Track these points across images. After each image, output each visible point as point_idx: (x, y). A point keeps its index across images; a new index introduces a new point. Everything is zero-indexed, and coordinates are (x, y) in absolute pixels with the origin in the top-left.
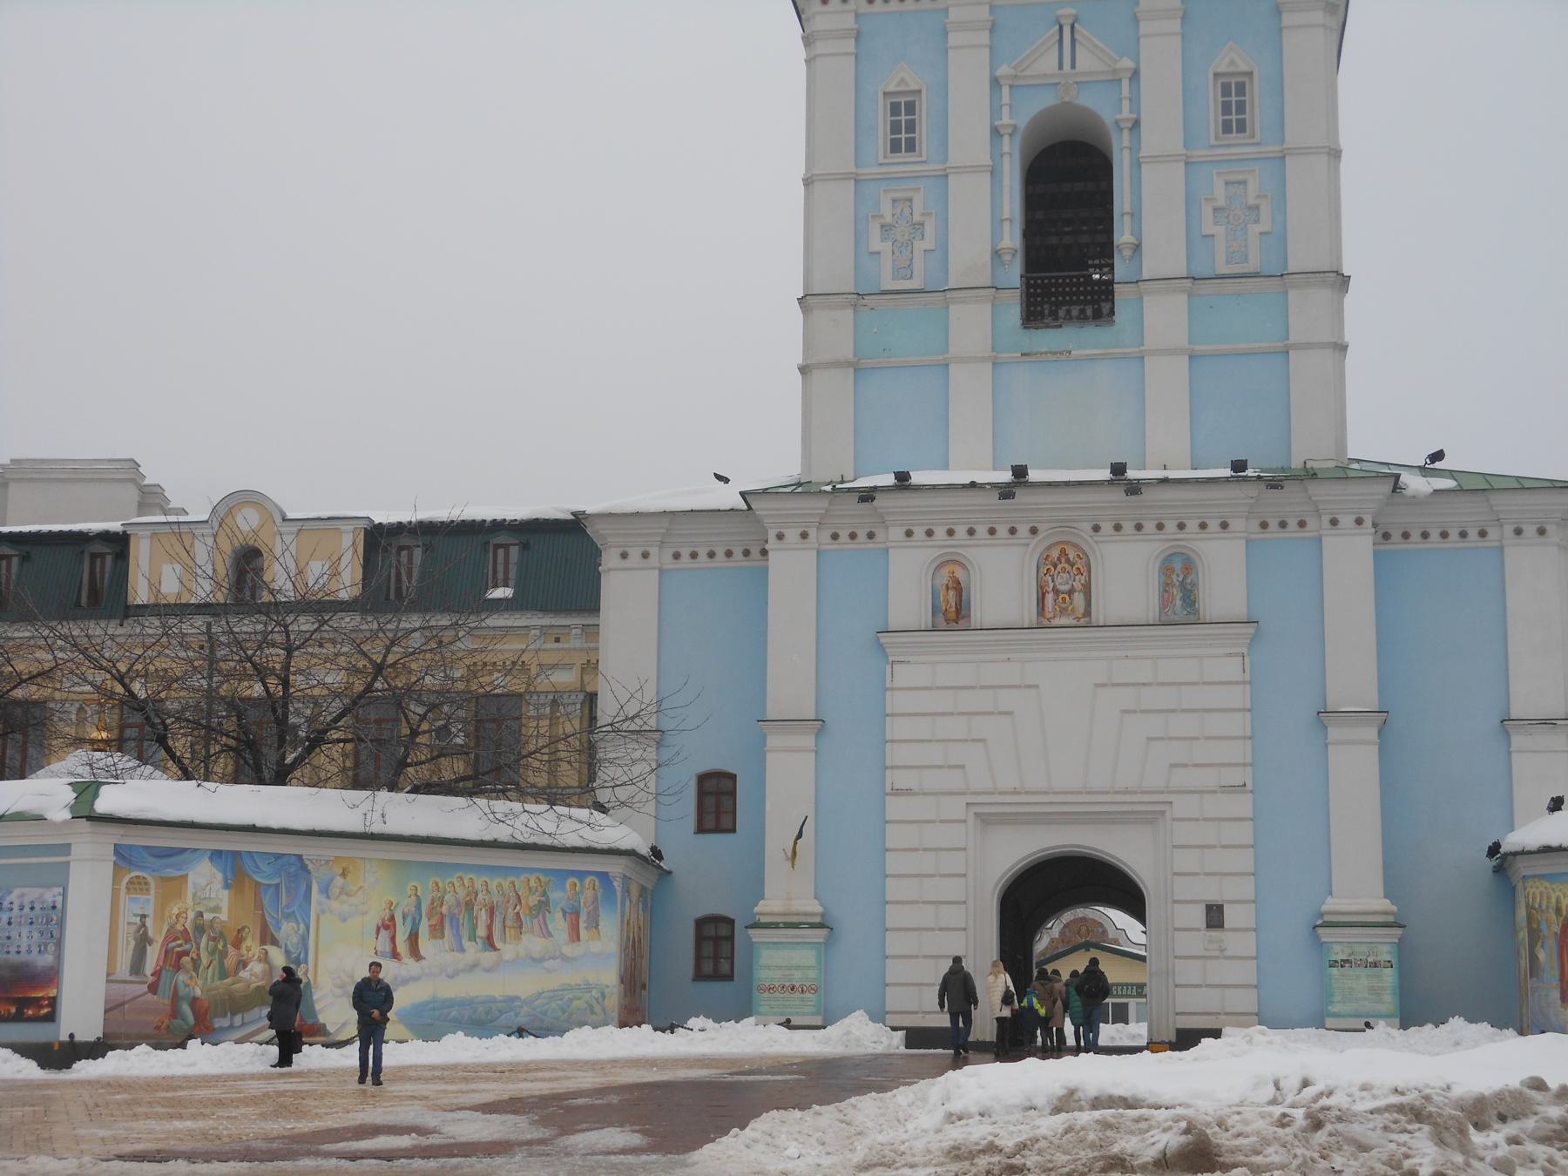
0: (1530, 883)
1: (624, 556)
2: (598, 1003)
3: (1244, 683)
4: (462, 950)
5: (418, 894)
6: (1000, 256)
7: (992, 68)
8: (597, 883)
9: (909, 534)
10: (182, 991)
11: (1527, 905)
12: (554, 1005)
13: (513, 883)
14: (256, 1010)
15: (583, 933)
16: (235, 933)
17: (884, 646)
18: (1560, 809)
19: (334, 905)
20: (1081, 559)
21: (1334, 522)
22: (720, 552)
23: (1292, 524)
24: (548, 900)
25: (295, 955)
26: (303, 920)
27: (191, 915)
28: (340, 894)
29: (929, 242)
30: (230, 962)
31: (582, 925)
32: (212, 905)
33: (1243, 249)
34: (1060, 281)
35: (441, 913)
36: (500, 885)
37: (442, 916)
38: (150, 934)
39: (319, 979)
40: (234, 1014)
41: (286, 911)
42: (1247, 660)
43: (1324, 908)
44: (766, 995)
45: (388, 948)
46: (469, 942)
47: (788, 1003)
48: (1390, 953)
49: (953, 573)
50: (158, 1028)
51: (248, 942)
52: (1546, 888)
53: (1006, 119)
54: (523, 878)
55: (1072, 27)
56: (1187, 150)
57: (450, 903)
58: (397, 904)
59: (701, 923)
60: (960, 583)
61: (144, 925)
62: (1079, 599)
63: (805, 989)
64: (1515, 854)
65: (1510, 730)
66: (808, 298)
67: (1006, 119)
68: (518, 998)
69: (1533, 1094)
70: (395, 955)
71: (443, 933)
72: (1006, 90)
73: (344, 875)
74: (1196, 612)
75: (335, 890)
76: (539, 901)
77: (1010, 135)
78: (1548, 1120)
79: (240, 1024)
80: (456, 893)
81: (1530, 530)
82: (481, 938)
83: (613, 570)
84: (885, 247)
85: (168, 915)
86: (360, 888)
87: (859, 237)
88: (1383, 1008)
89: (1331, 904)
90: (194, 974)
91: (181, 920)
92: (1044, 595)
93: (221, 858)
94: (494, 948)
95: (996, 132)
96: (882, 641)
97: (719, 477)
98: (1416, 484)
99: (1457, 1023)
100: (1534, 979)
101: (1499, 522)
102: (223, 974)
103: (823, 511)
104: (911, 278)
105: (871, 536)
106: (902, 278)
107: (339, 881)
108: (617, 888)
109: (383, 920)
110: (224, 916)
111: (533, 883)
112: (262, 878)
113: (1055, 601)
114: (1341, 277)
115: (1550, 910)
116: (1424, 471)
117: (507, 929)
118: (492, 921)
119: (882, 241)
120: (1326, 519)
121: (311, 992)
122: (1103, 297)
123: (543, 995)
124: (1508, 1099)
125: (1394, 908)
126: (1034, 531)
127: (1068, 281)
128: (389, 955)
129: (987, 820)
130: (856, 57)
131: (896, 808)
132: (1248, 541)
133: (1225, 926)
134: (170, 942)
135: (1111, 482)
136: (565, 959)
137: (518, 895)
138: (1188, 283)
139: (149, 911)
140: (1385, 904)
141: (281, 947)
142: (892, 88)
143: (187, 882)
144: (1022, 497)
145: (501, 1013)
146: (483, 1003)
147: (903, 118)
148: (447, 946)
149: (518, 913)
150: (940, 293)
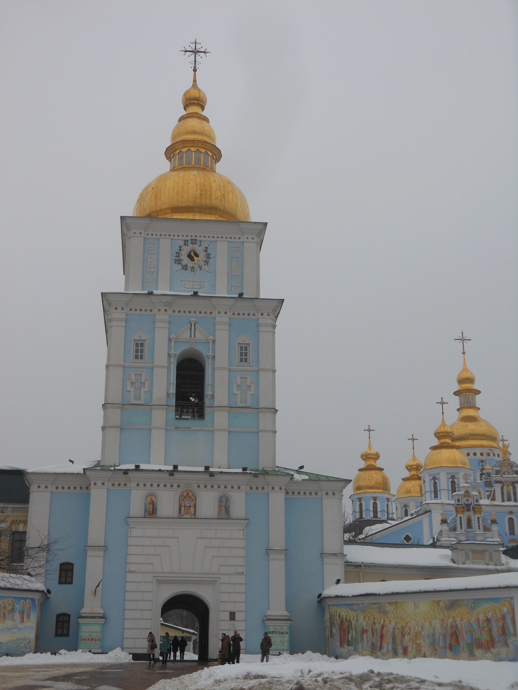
0: (331, 607)
1: (39, 487)
3: (244, 539)
6: (169, 395)
7: (169, 335)
8: (31, 602)
9: (138, 485)
11: (330, 614)
13: (4, 602)
15: (25, 620)
17: (128, 522)
18: (339, 583)
20: (193, 496)
21: (273, 488)
22: (72, 487)
23: (260, 488)
29: (146, 389)
31: (25, 616)
33: (245, 399)
34: (185, 404)
42: (245, 531)
43: (267, 614)
44: (83, 642)
47: (90, 645)
48: (287, 629)
49: (152, 499)
52: (336, 609)
53: (173, 352)
55: (195, 324)
56: (229, 366)
59: (58, 616)
60: (154, 502)
62: (192, 509)
63: (96, 640)
64: (327, 598)
65: (324, 557)
66: (106, 404)
67: (173, 352)
69: (371, 674)
72: (173, 343)
74: (229, 515)
77: (174, 357)
78: (376, 681)
81: (330, 493)
83: (35, 492)
84: (132, 389)
87: (124, 386)
88: (285, 648)
89: (269, 613)
92: (181, 507)
95: (169, 355)
96: (128, 520)
97: (70, 461)
98: (297, 477)
99: (309, 653)
100: (332, 638)
101: (321, 490)
103: (110, 476)
104: (140, 400)
105: (125, 485)
106: (137, 400)
108: (37, 603)
113: (185, 509)
114: (275, 410)
115: (337, 616)
116: (298, 472)
119: (131, 387)
120: (271, 487)
122: (190, 407)
123: (11, 642)
124: (366, 676)
125: (289, 614)
126: (179, 486)
127: (188, 404)
129: (160, 582)
130: (125, 328)
131: (130, 577)
132: (246, 493)
133: (236, 620)
135: (204, 472)
136: (19, 629)
138: (228, 409)
140: (286, 613)
142: (136, 338)
144: (176, 475)
147: (140, 348)
149: (4, 613)
150: (149, 406)
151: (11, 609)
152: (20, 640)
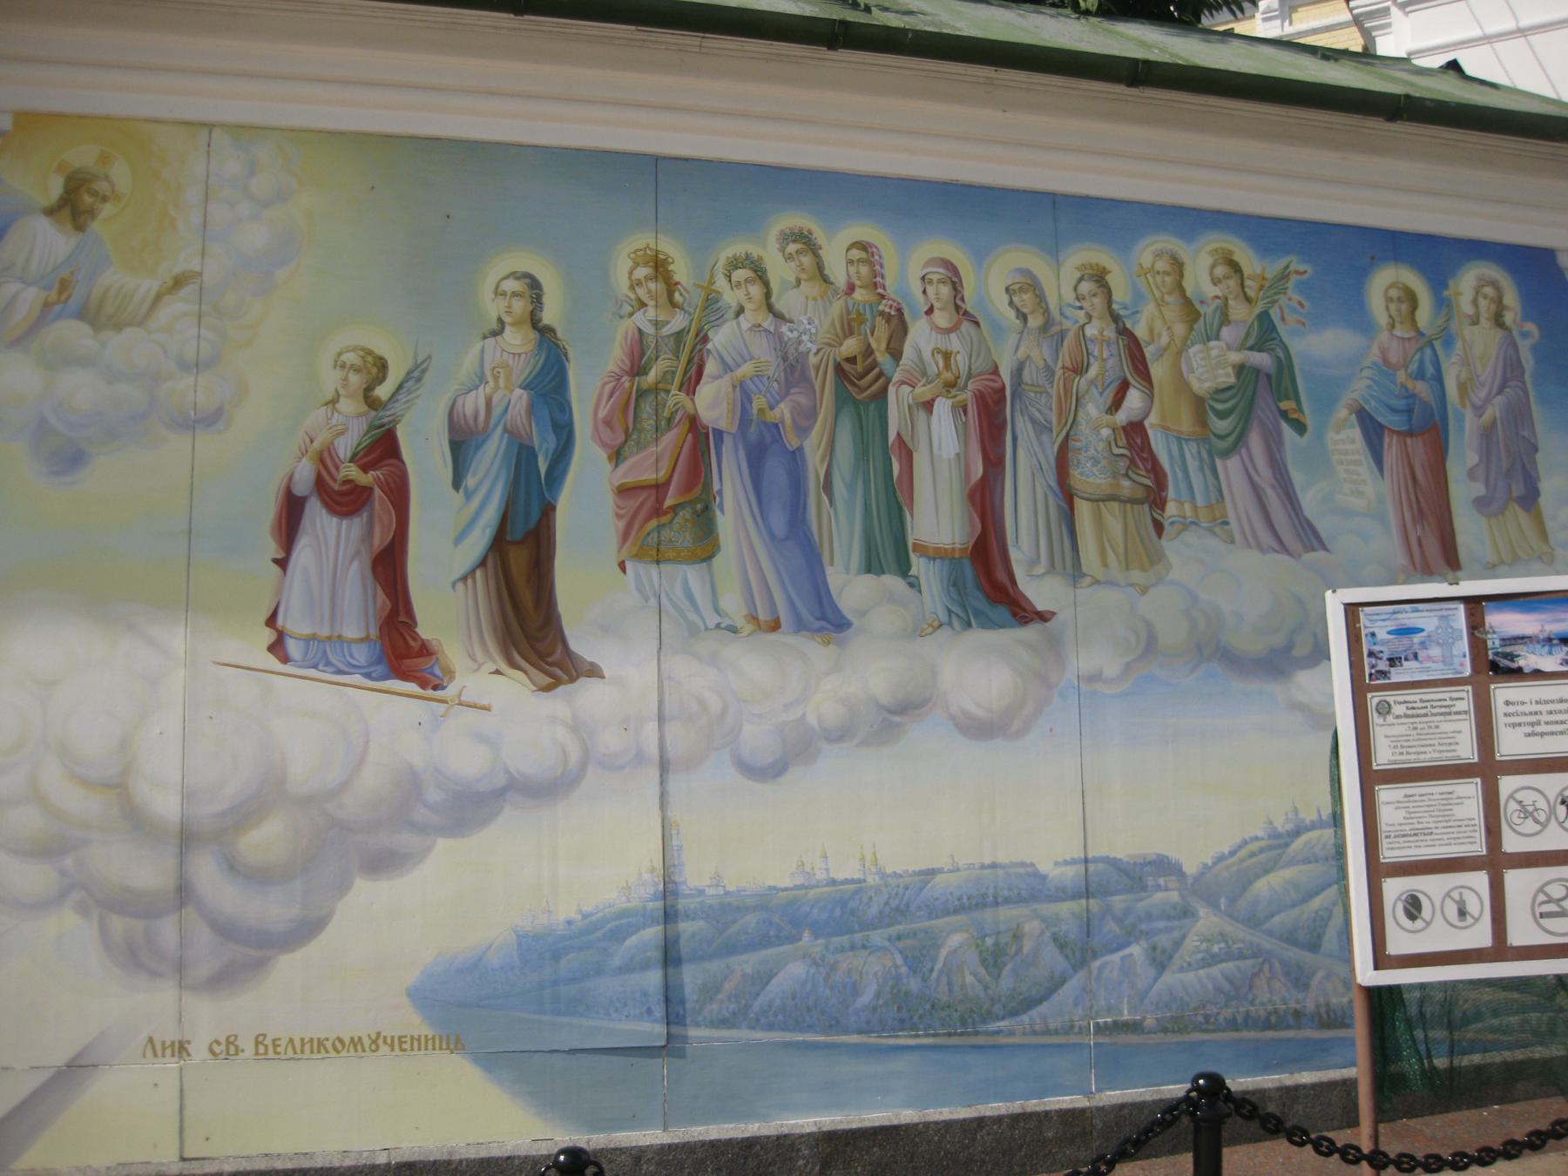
5: (549, 316)
8: (1511, 298)
13: (1100, 278)
15: (1469, 528)
24: (1285, 367)
28: (46, 313)
31: (1462, 491)
35: (694, 422)
36: (1032, 285)
37: (700, 438)
46: (869, 579)
54: (1150, 249)
57: (746, 369)
58: (415, 374)
68: (1164, 866)
76: (1240, 369)
80: (778, 316)
82: (934, 554)
86: (178, 283)
94: (1022, 612)
109: (325, 459)
111: (1201, 278)
117: (1083, 509)
118: (994, 463)
123: (1298, 843)
128: (361, 655)
137: (1124, 332)
146: (974, 902)
148: (733, 604)
149: (1135, 430)
151: (1227, 377)
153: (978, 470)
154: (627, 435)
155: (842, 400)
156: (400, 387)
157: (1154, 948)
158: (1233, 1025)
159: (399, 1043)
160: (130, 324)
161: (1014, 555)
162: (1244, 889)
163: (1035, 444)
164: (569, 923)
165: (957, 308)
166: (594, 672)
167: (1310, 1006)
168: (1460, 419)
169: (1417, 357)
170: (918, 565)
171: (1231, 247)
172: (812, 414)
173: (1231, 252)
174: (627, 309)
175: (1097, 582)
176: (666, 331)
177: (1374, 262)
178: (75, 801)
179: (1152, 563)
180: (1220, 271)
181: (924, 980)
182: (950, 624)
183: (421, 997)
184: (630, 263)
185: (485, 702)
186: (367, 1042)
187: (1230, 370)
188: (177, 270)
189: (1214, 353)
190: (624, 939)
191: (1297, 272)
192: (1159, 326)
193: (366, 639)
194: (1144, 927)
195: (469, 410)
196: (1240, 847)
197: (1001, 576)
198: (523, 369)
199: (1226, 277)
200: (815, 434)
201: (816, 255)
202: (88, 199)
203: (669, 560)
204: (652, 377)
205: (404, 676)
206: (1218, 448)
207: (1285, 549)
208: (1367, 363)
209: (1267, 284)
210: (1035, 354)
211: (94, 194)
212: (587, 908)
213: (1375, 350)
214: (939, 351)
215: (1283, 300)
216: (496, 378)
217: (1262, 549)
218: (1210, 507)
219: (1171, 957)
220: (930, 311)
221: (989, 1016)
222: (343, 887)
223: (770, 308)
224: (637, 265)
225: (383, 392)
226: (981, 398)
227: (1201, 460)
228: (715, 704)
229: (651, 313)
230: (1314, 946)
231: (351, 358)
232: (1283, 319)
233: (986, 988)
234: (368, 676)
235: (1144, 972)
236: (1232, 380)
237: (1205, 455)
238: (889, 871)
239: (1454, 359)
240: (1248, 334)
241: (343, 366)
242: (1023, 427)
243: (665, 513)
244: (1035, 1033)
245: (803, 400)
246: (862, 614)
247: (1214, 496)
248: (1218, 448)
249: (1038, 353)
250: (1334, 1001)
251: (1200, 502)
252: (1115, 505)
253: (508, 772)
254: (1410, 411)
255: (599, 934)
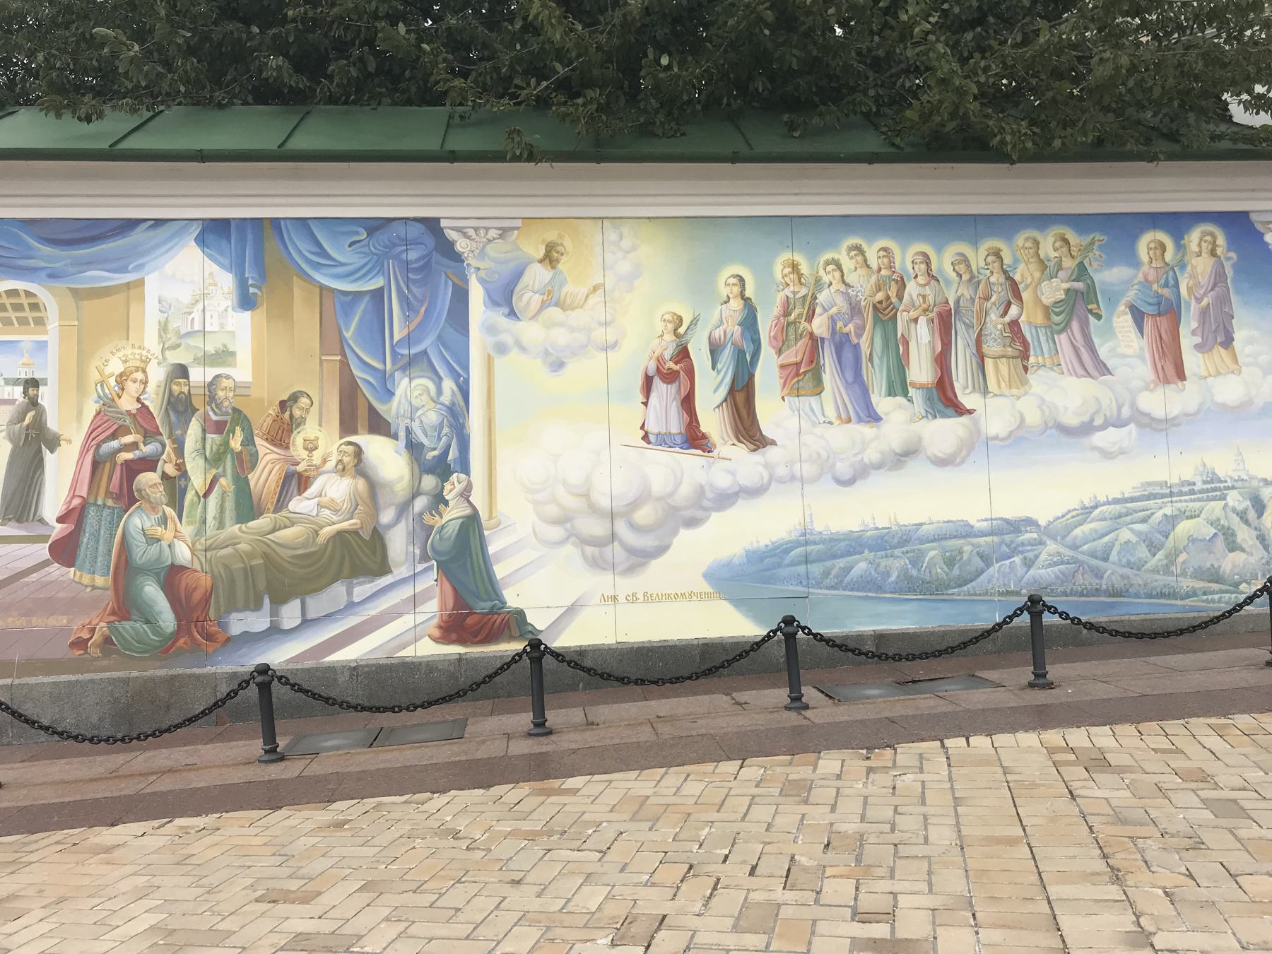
2: (1247, 522)
4: (872, 416)
5: (748, 293)
8: (1221, 240)
10: (142, 553)
12: (1125, 535)
13: (997, 254)
14: (339, 589)
15: (1191, 360)
16: (273, 411)
19: (530, 331)
24: (1091, 288)
25: (435, 453)
26: (452, 370)
27: (157, 375)
28: (544, 306)
30: (264, 477)
31: (1187, 342)
32: (210, 349)
35: (811, 334)
36: (965, 260)
37: (815, 343)
38: (52, 424)
39: (503, 505)
40: (279, 600)
41: (405, 352)
45: (675, 425)
46: (890, 398)
50: (80, 644)
51: (310, 429)
54: (1021, 239)
57: (834, 310)
58: (694, 322)
61: (34, 403)
68: (1030, 523)
70: (694, 439)
71: (818, 382)
73: (550, 257)
75: (527, 298)
76: (1068, 291)
79: (298, 621)
80: (847, 285)
82: (919, 387)
85: (96, 376)
86: (595, 289)
90: (170, 512)
91: (133, 388)
93: (229, 239)
94: (960, 410)
102: (247, 508)
107: (537, 275)
109: (660, 360)
110: (242, 371)
112: (338, 277)
117: (989, 363)
121: (481, 536)
123: (1096, 512)
128: (679, 440)
134: (104, 441)
136: (1147, 422)
137: (1009, 278)
139: (48, 370)
141: (395, 437)
143: (142, 298)
145: (987, 559)
148: (831, 413)
149: (1014, 325)
152: (1171, 494)
153: (939, 348)
154: (784, 343)
155: (877, 320)
156: (688, 328)
157: (1025, 558)
158: (1065, 594)
159: (702, 596)
160: (577, 308)
161: (956, 385)
162: (1069, 533)
163: (966, 333)
164: (766, 546)
165: (929, 274)
166: (773, 443)
167: (1104, 587)
168: (1188, 308)
169: (1165, 276)
170: (912, 392)
171: (1063, 232)
172: (864, 328)
173: (1064, 234)
174: (781, 287)
175: (996, 395)
176: (798, 296)
177: (1142, 231)
178: (572, 503)
179: (1022, 385)
180: (1058, 244)
181: (919, 570)
182: (927, 417)
183: (708, 576)
184: (782, 267)
185: (729, 457)
186: (687, 595)
187: (1062, 292)
188: (594, 283)
189: (1054, 284)
190: (789, 553)
191: (1098, 241)
192: (1027, 274)
193: (680, 433)
194: (1020, 549)
195: (717, 337)
196: (1067, 514)
197: (950, 395)
198: (739, 317)
199: (1061, 247)
200: (865, 336)
201: (864, 256)
202: (555, 255)
203: (802, 395)
204: (792, 317)
205: (696, 448)
206: (1054, 330)
207: (1089, 375)
208: (1136, 282)
209: (1082, 248)
210: (966, 293)
211: (558, 252)
212: (774, 539)
213: (1141, 275)
214: (920, 295)
215: (1091, 255)
216: (727, 322)
217: (1077, 376)
218: (1051, 357)
219: (1034, 563)
220: (916, 277)
221: (948, 587)
222: (675, 533)
223: (843, 282)
224: (785, 267)
225: (681, 330)
226: (940, 315)
227: (1047, 336)
228: (824, 455)
229: (792, 288)
230: (1106, 559)
231: (668, 317)
232: (1091, 265)
233: (947, 575)
234: (681, 448)
235: (1020, 570)
236: (1063, 297)
237: (1049, 334)
238: (902, 524)
239: (1186, 275)
240: (1072, 273)
241: (665, 320)
242: (961, 327)
243: (800, 375)
244: (970, 595)
245: (858, 321)
246: (887, 414)
247: (1053, 352)
248: (1054, 330)
249: (966, 292)
250: (1116, 586)
251: (1046, 356)
252: (1004, 359)
253: (740, 485)
254: (1159, 304)
255: (779, 551)
